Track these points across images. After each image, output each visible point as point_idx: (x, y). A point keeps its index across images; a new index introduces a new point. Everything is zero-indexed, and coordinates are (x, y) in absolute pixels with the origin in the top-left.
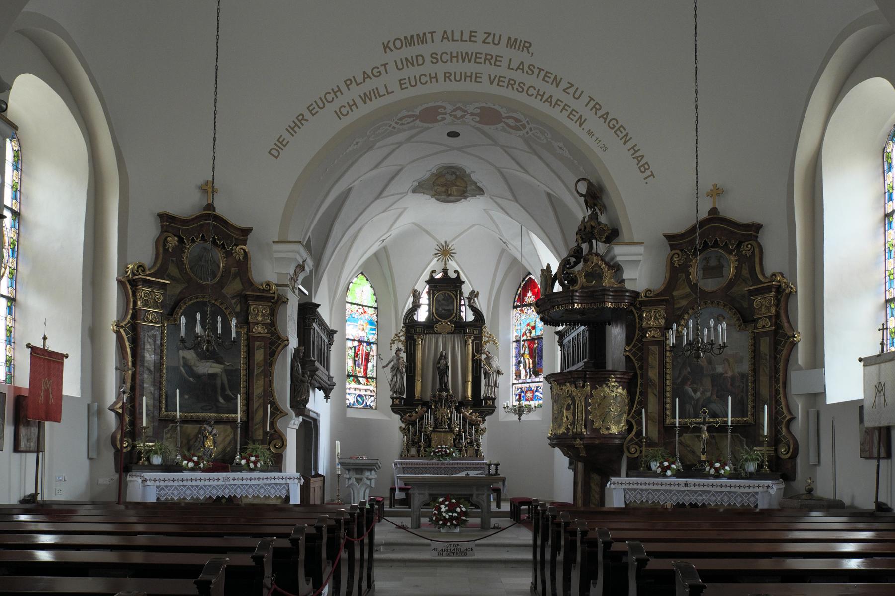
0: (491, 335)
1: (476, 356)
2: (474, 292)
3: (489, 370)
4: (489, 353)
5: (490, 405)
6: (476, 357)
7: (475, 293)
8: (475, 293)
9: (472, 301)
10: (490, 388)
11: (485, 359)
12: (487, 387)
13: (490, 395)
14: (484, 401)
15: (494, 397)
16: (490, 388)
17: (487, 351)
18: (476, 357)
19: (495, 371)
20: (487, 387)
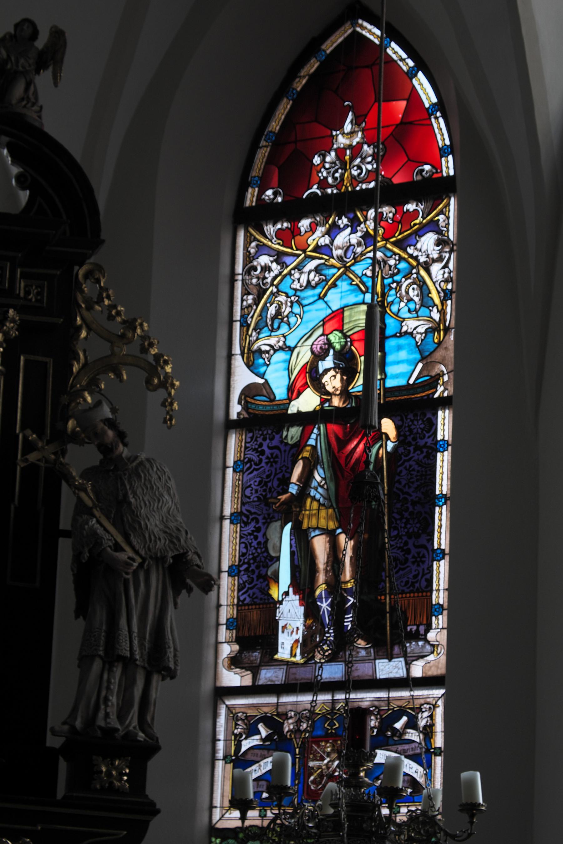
0: (130, 325)
1: (29, 447)
2: (35, 35)
3: (117, 548)
4: (121, 436)
5: (111, 789)
6: (33, 457)
7: (40, 43)
8: (40, 43)
9: (19, 90)
10: (118, 671)
11: (87, 474)
12: (97, 665)
13: (114, 722)
14: (63, 765)
15: (141, 736)
16: (118, 671)
17: (111, 423)
18: (33, 457)
19: (160, 560)
20: (97, 665)
